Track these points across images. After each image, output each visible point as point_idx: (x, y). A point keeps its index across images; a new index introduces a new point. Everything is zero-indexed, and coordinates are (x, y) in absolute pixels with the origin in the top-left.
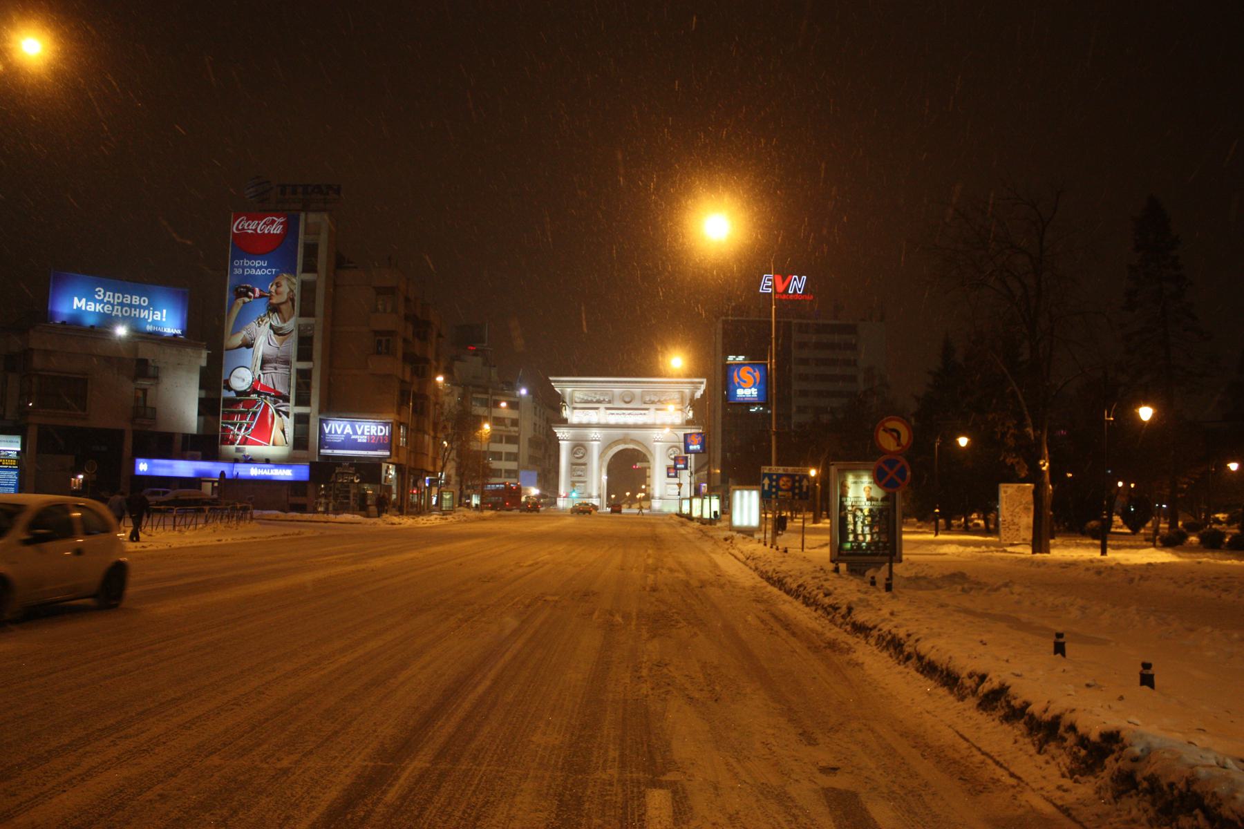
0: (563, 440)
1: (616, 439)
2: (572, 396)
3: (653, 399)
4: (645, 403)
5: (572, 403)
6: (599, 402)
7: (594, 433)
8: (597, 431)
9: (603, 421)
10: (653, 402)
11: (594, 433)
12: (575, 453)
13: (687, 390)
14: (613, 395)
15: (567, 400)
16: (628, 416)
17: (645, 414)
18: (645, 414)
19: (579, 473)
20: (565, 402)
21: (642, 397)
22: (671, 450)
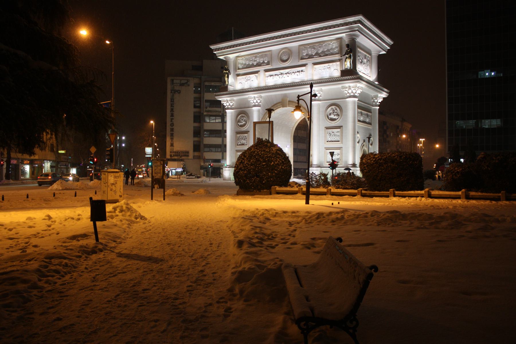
0: (228, 109)
1: (275, 103)
2: (236, 63)
3: (310, 53)
4: (302, 59)
5: (236, 71)
6: (259, 65)
7: (253, 98)
8: (256, 95)
9: (263, 84)
10: (310, 57)
11: (253, 98)
12: (239, 121)
13: (344, 35)
14: (271, 55)
16: (285, 75)
17: (302, 71)
18: (302, 71)
19: (243, 141)
21: (299, 52)
22: (330, 108)
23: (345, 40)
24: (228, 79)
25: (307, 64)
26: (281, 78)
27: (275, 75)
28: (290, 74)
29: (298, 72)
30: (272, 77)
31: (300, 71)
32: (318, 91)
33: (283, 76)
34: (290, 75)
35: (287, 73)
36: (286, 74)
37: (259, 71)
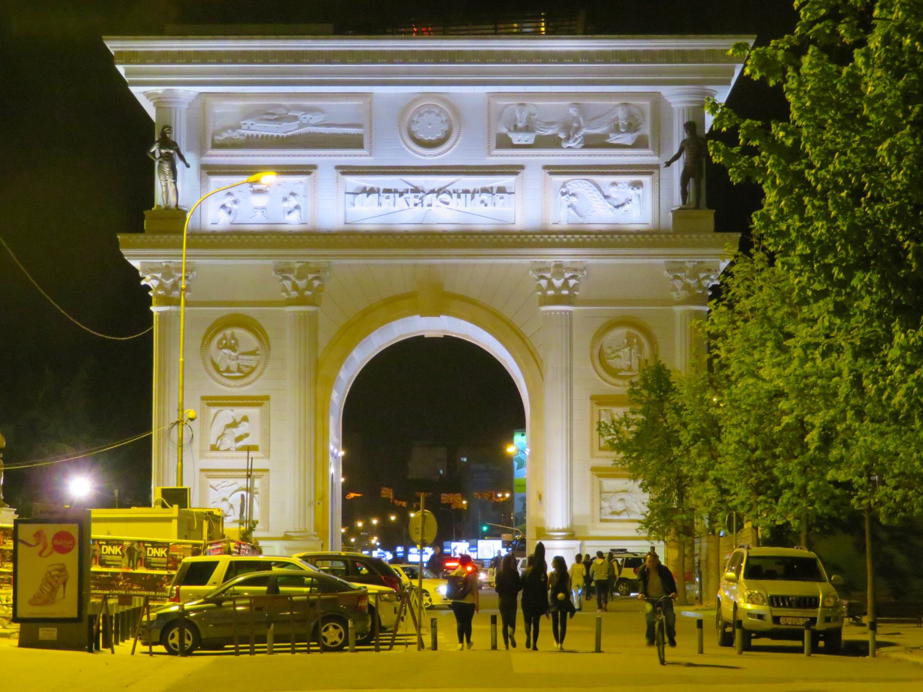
4: (504, 143)
14: (371, 111)
15: (181, 136)
17: (501, 190)
18: (501, 190)
20: (173, 145)
23: (670, 103)
24: (175, 183)
25: (522, 167)
26: (416, 205)
27: (387, 191)
28: (455, 196)
29: (485, 191)
30: (374, 197)
31: (492, 188)
32: (576, 270)
33: (421, 199)
34: (454, 201)
35: (440, 190)
36: (432, 192)
37: (314, 167)
